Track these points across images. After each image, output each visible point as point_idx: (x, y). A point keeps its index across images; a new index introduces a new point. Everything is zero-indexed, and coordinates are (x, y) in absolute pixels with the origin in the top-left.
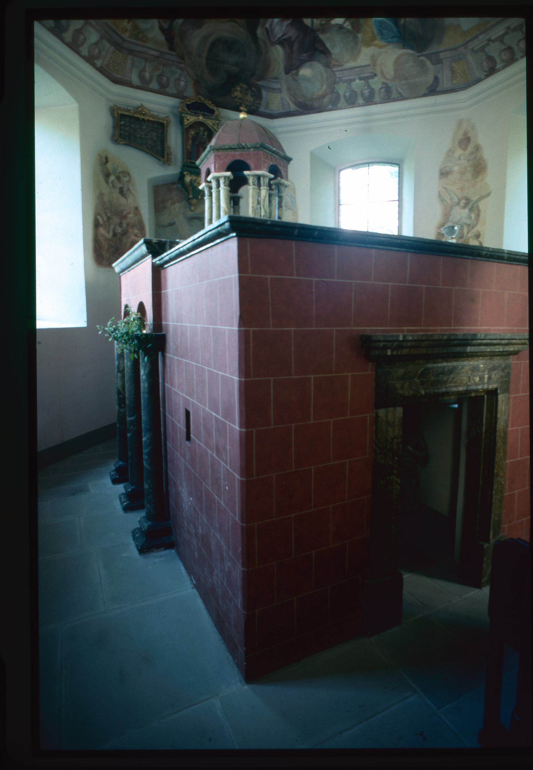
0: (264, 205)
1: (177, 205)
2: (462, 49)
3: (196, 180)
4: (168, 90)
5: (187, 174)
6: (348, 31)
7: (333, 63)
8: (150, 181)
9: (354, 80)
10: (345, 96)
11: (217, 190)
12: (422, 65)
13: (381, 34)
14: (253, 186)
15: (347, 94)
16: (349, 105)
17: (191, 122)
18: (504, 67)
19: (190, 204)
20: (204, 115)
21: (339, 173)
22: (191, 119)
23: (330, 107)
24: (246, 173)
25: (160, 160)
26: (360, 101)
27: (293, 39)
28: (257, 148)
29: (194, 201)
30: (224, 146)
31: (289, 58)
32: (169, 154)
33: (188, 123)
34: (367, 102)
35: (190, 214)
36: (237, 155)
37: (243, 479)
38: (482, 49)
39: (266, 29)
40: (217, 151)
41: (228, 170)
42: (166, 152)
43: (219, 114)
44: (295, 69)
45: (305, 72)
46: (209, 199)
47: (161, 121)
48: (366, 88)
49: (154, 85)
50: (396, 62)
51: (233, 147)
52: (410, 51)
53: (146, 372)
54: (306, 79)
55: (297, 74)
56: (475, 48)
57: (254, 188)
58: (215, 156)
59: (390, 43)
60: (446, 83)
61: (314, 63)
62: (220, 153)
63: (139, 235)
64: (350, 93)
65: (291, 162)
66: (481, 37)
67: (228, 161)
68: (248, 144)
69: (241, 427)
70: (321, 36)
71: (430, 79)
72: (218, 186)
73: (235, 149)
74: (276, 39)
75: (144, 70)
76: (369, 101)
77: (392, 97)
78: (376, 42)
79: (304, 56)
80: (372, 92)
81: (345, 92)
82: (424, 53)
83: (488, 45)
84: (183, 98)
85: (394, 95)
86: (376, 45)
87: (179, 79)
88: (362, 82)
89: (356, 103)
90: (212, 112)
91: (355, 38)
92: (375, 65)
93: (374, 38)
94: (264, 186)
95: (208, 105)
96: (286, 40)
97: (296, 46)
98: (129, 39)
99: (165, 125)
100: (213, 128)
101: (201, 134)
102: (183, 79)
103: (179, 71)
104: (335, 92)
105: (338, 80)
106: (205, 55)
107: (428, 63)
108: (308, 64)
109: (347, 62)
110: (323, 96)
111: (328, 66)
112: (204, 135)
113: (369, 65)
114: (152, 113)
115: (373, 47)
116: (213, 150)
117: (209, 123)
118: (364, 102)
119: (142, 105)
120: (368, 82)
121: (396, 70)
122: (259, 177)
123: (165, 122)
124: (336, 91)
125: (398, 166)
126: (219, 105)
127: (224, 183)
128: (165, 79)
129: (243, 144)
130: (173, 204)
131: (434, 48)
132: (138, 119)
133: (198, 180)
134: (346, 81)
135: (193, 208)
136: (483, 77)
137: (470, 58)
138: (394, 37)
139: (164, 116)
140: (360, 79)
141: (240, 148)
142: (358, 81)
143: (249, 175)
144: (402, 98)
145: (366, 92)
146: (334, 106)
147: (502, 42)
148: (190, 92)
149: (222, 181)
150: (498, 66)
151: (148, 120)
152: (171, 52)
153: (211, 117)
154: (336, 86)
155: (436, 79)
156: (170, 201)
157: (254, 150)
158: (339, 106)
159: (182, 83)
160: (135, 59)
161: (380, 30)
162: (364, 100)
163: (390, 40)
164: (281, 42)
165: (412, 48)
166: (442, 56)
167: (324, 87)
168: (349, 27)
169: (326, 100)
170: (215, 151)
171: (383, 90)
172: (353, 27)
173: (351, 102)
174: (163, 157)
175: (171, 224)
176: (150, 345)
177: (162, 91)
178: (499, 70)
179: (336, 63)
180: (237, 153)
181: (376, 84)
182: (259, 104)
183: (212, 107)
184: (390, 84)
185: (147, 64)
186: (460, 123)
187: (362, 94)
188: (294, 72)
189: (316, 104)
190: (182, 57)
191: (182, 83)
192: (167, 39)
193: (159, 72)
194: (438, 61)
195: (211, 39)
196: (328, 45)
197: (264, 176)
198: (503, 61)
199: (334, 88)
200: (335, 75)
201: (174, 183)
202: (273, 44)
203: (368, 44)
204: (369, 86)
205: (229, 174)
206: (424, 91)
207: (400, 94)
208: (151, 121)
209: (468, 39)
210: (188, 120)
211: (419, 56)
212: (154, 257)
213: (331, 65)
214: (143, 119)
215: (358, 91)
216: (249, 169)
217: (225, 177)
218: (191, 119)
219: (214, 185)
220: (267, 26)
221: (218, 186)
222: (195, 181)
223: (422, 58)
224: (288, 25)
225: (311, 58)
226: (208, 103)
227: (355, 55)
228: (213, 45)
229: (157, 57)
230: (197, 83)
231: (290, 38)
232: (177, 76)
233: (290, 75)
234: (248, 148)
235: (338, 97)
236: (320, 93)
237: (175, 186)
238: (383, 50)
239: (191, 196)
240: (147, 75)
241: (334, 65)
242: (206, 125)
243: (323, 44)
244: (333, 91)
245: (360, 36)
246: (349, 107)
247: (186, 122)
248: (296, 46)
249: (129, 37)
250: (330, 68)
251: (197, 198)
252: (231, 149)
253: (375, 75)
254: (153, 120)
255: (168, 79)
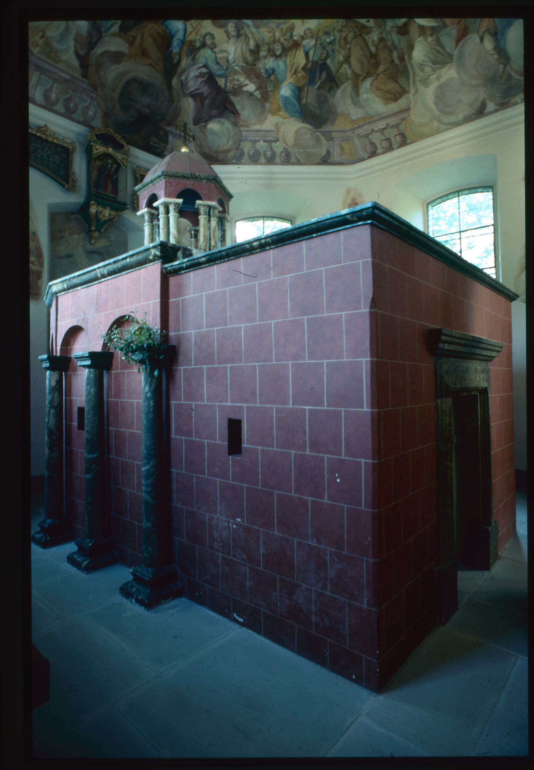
0: (214, 236)
1: (76, 237)
2: (350, 133)
3: (102, 211)
4: (74, 116)
5: (93, 204)
6: (257, 99)
7: (241, 123)
8: (50, 206)
9: (259, 141)
10: (249, 154)
11: (166, 216)
12: (318, 139)
13: (286, 107)
14: (205, 216)
15: (251, 152)
16: (252, 162)
17: (100, 152)
18: (384, 153)
19: (91, 237)
20: (114, 148)
21: (235, 224)
22: (99, 149)
23: (234, 161)
24: (198, 202)
25: (63, 186)
26: (263, 160)
27: (205, 95)
28: (210, 180)
29: (96, 234)
30: (177, 173)
31: (199, 110)
32: (74, 181)
33: (97, 153)
34: (268, 162)
35: (90, 247)
36: (190, 184)
37: (374, 461)
38: (367, 136)
39: (181, 81)
40: (168, 177)
41: (178, 197)
42: (70, 179)
43: (129, 149)
44: (203, 122)
45: (214, 126)
46: (149, 225)
47: (65, 145)
48: (268, 149)
49: (60, 107)
50: (297, 132)
51: (186, 176)
52: (308, 126)
53: (152, 389)
54: (213, 133)
55: (205, 127)
56: (361, 134)
57: (205, 218)
58: (166, 182)
59: (292, 116)
60: (336, 156)
61: (223, 120)
62: (171, 180)
63: (36, 263)
64: (253, 151)
65: (232, 200)
66: (366, 127)
67: (180, 189)
68: (201, 175)
69: (372, 407)
70: (233, 98)
71: (324, 152)
72: (167, 212)
73: (188, 178)
74: (189, 91)
75: (51, 89)
76: (271, 161)
77: (291, 161)
78: (281, 113)
79: (214, 112)
80: (274, 154)
81: (249, 151)
82: (319, 130)
83: (371, 133)
84: (92, 128)
85: (293, 160)
86: (280, 116)
87: (87, 108)
88: (266, 144)
89: (258, 161)
90: (122, 147)
91: (263, 106)
92: (278, 132)
93: (279, 110)
94: (214, 217)
95: (118, 139)
96: (197, 94)
97: (207, 102)
98: (39, 55)
99: (71, 151)
100: (122, 162)
101: (109, 166)
102: (92, 108)
103: (89, 100)
104: (240, 149)
105: (243, 138)
106: (118, 90)
107: (323, 139)
108: (217, 120)
109: (254, 124)
110: (229, 151)
111: (235, 124)
112: (112, 167)
113: (273, 131)
114: (56, 136)
115: (278, 117)
116: (165, 175)
117: (119, 156)
118: (266, 162)
119: (46, 126)
120: (271, 145)
121: (296, 140)
122: (210, 207)
123: (71, 147)
124: (240, 148)
125: (290, 222)
126: (130, 143)
127: (175, 209)
128: (72, 105)
129: (197, 174)
130: (71, 234)
131: (327, 128)
132: (40, 138)
133: (104, 212)
134: (251, 141)
135: (93, 242)
136: (367, 157)
137: (356, 141)
138: (296, 112)
139: (69, 141)
140: (265, 141)
141: (192, 178)
142: (262, 143)
143: (201, 205)
144: (299, 163)
145: (269, 154)
146: (238, 160)
147: (383, 133)
148: (98, 123)
149: (171, 208)
150: (378, 151)
151: (52, 143)
152: (83, 79)
153: (120, 151)
154: (241, 143)
155: (328, 152)
156: (68, 232)
157: (207, 182)
158: (243, 161)
159: (91, 113)
160: (42, 76)
161: (285, 104)
162: (266, 160)
163: (293, 114)
164: (194, 95)
165: (311, 124)
166: (334, 135)
167: (230, 143)
168: (259, 96)
169: (230, 155)
170: (166, 177)
171: (284, 154)
172: (262, 97)
173: (254, 159)
174: (67, 182)
175: (69, 256)
176: (162, 357)
177: (68, 114)
178: (379, 154)
179: (244, 124)
180: (189, 182)
181: (278, 147)
182: (165, 148)
183: (122, 142)
184: (290, 150)
185: (55, 85)
186: (348, 191)
187: (265, 155)
188: (203, 124)
189: (221, 157)
190: (94, 87)
191: (91, 113)
192: (81, 66)
193: (67, 96)
194: (330, 139)
195: (127, 78)
196: (238, 107)
197: (214, 208)
198: (382, 148)
199: (239, 145)
200: (241, 133)
201: (73, 213)
202: (185, 95)
203: (274, 114)
204: (271, 149)
205: (180, 201)
206: (318, 161)
207: (298, 159)
208: (55, 144)
209: (356, 126)
210: (97, 149)
211: (315, 132)
212: (163, 263)
213: (239, 125)
214: (46, 140)
215: (262, 151)
216: (200, 199)
217: (176, 204)
218: (99, 149)
219: (162, 210)
220: (183, 78)
221: (167, 212)
222: (101, 213)
223: (317, 133)
224: (202, 82)
225: (220, 115)
226: (118, 137)
227: (261, 120)
228: (129, 82)
229: (66, 80)
230: (106, 116)
231: (202, 94)
232: (86, 104)
233: (198, 126)
234: (201, 179)
235: (242, 154)
236: (225, 147)
237: (74, 217)
238: (286, 120)
239: (93, 228)
240: (53, 96)
241: (241, 125)
242: (115, 158)
243: (233, 105)
244: (238, 148)
245: (267, 105)
246: (252, 163)
247: (95, 152)
248: (207, 102)
249: (38, 53)
250: (237, 127)
251: (99, 231)
252: (184, 177)
253: (278, 140)
254: (57, 142)
255: (76, 105)
